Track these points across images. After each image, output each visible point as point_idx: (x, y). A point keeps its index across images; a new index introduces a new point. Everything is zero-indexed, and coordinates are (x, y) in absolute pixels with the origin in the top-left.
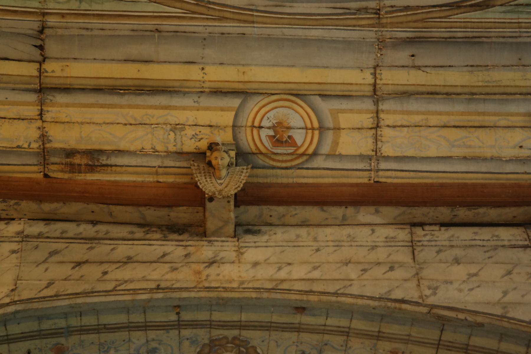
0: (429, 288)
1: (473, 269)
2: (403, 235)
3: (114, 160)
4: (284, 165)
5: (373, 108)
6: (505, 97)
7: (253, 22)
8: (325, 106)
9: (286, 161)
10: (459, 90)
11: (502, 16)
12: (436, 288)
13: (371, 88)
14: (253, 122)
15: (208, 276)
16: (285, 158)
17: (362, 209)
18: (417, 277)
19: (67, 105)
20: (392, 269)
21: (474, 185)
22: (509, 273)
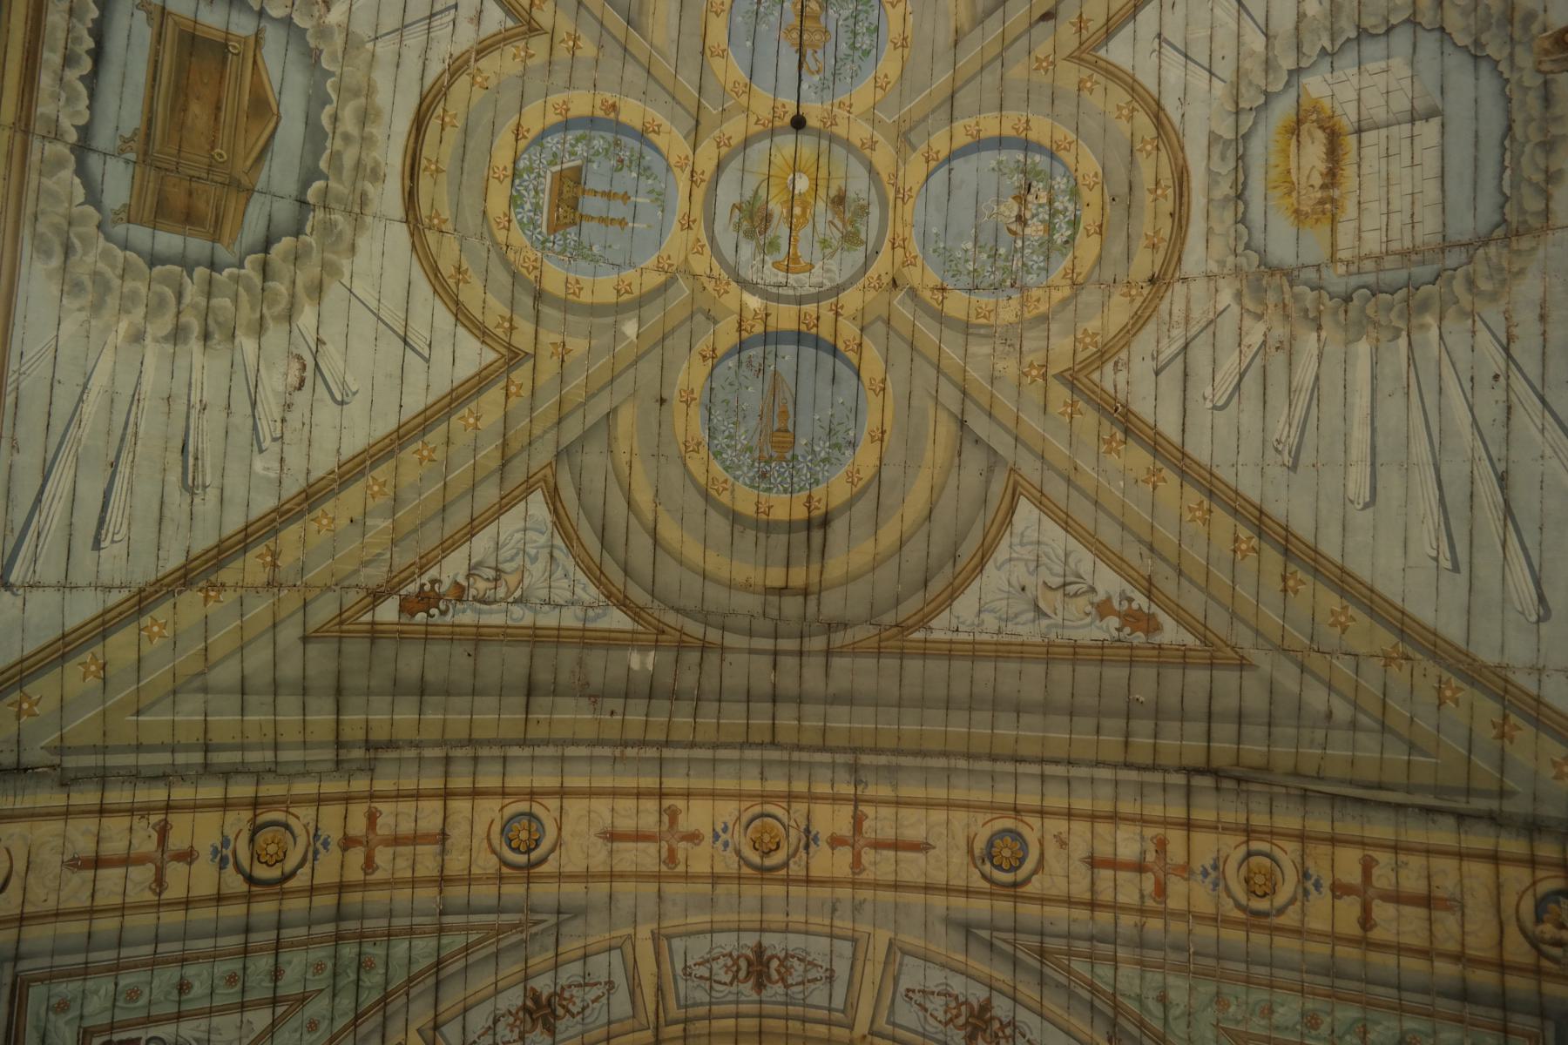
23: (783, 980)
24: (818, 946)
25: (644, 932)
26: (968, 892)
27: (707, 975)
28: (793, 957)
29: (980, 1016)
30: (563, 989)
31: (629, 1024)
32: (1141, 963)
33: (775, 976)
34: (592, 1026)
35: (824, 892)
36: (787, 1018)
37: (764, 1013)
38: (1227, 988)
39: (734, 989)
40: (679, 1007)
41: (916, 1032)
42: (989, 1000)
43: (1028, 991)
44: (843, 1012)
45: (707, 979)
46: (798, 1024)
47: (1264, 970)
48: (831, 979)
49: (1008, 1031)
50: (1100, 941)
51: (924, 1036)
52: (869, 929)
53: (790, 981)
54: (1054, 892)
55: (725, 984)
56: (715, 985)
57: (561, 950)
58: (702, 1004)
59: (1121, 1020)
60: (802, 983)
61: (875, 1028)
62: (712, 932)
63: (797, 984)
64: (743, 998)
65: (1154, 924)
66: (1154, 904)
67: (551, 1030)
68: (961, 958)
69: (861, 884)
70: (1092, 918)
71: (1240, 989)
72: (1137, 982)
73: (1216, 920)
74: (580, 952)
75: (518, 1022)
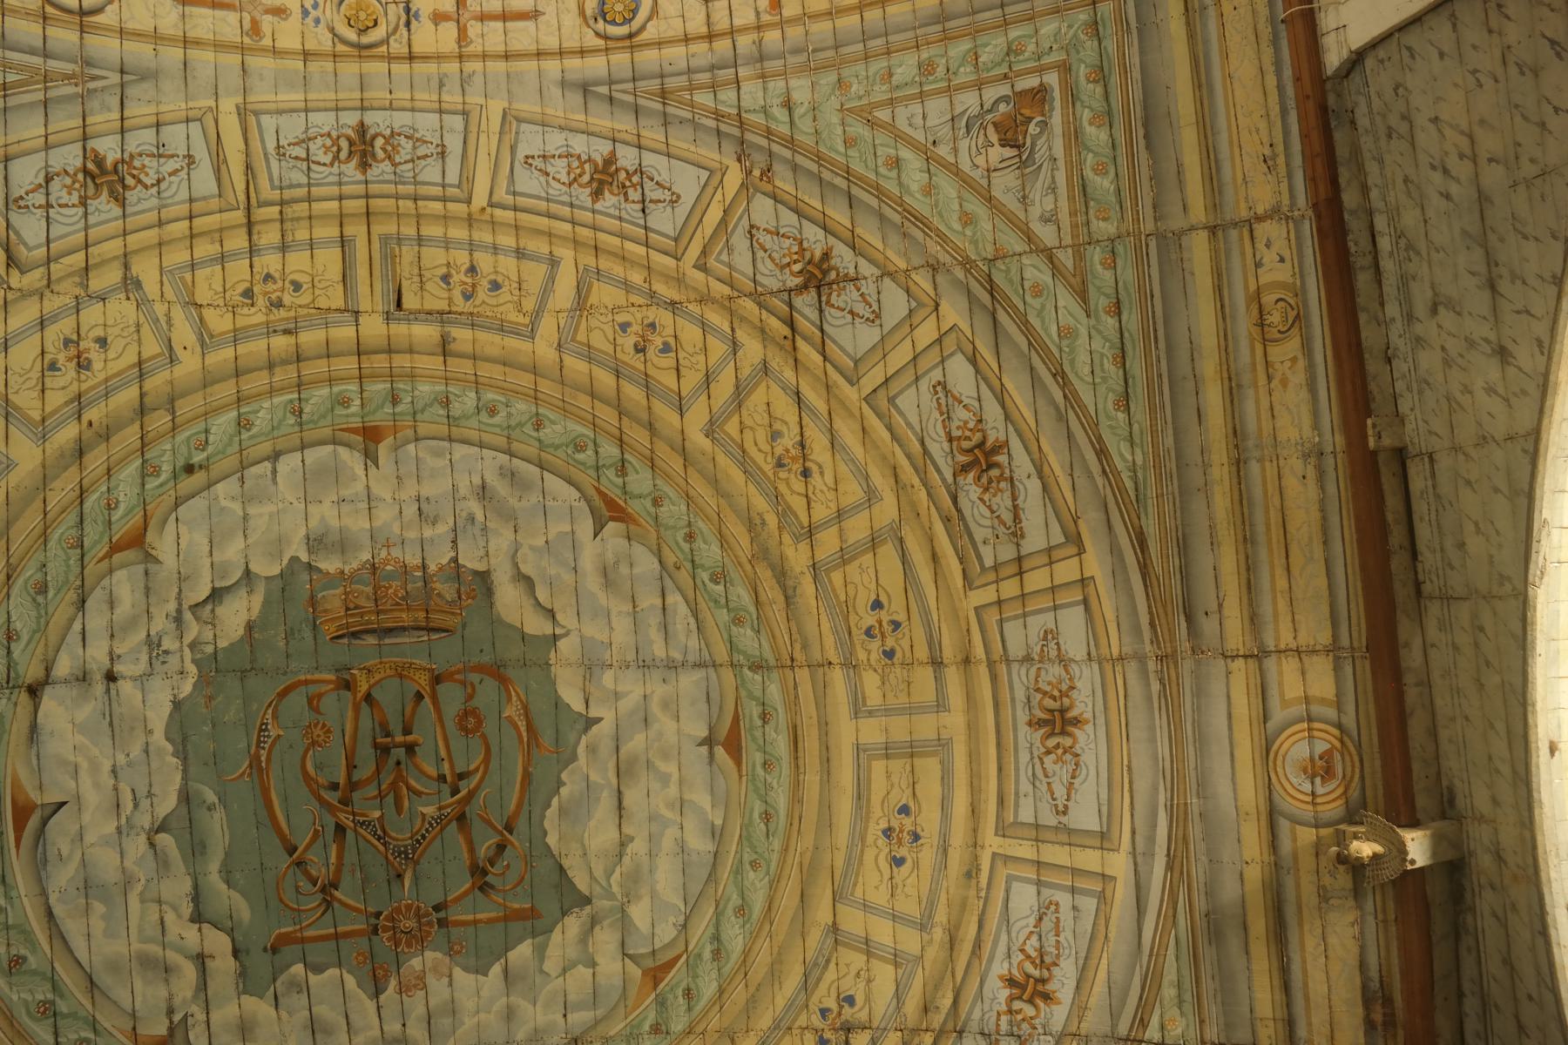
0: (1502, 584)
1: (1469, 528)
2: (1434, 610)
3: (1374, 973)
4: (1357, 764)
5: (1274, 657)
6: (1245, 502)
7: (1186, 804)
8: (1278, 715)
9: (1352, 761)
10: (1242, 557)
11: (1150, 517)
12: (1501, 575)
13: (1250, 661)
14: (1307, 803)
15: (1518, 866)
16: (1349, 764)
17: (1404, 665)
18: (1488, 597)
19: (1310, 1024)
20: (1481, 629)
21: (1358, 530)
22: (1468, 483)
23: (389, 157)
24: (427, 123)
25: (228, 105)
26: (582, 52)
27: (304, 155)
28: (399, 135)
29: (604, 171)
30: (132, 156)
31: (214, 204)
32: (763, 76)
33: (380, 154)
34: (169, 201)
35: (431, 68)
36: (397, 197)
37: (371, 192)
38: (845, 72)
39: (335, 169)
40: (273, 188)
41: (538, 198)
42: (613, 153)
43: (653, 134)
44: (459, 186)
45: (303, 160)
46: (410, 204)
47: (880, 41)
48: (443, 154)
49: (635, 179)
50: (720, 68)
51: (548, 200)
52: (481, 101)
53: (398, 159)
54: (671, 33)
55: (324, 164)
56: (313, 166)
57: (126, 114)
58: (299, 186)
59: (749, 136)
60: (412, 161)
61: (495, 199)
62: (306, 110)
63: (405, 162)
64: (346, 179)
65: (772, 37)
66: (769, 18)
67: (122, 202)
68: (582, 117)
69: (469, 56)
70: (711, 49)
71: (860, 68)
72: (761, 94)
73: (831, 13)
74: (153, 119)
75: (77, 185)
